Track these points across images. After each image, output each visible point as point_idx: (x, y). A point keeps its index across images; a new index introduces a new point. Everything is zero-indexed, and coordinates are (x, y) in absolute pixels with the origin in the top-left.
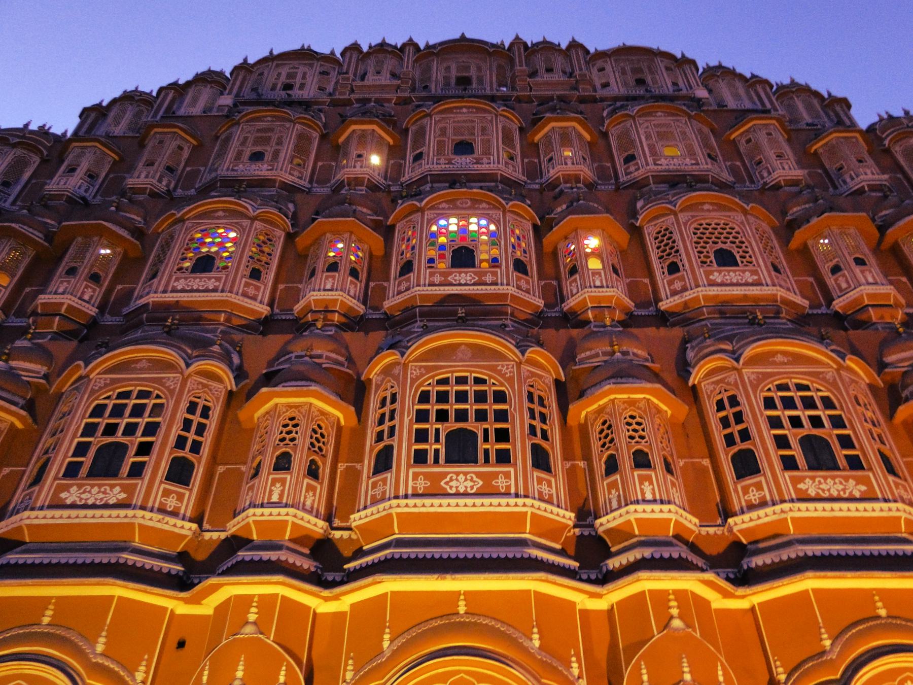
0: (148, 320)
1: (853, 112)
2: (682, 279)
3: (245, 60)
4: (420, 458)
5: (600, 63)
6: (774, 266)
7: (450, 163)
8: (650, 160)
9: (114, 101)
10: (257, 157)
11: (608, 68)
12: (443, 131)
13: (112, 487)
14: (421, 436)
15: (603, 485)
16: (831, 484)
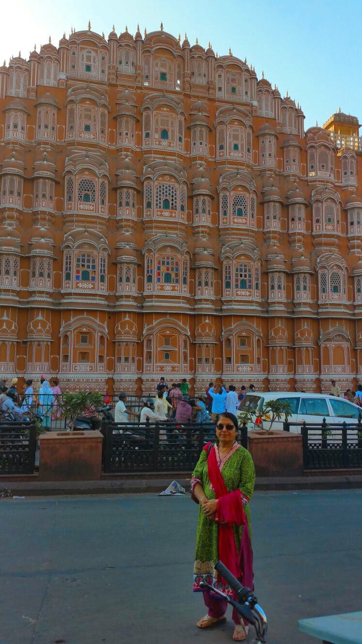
0: (77, 221)
1: (305, 120)
2: (226, 219)
3: (64, 36)
4: (159, 280)
5: (220, 72)
6: (253, 214)
7: (159, 144)
8: (228, 152)
9: (11, 67)
10: (87, 128)
11: (223, 76)
12: (157, 124)
13: (89, 284)
14: (159, 274)
15: (197, 288)
16: (243, 292)
